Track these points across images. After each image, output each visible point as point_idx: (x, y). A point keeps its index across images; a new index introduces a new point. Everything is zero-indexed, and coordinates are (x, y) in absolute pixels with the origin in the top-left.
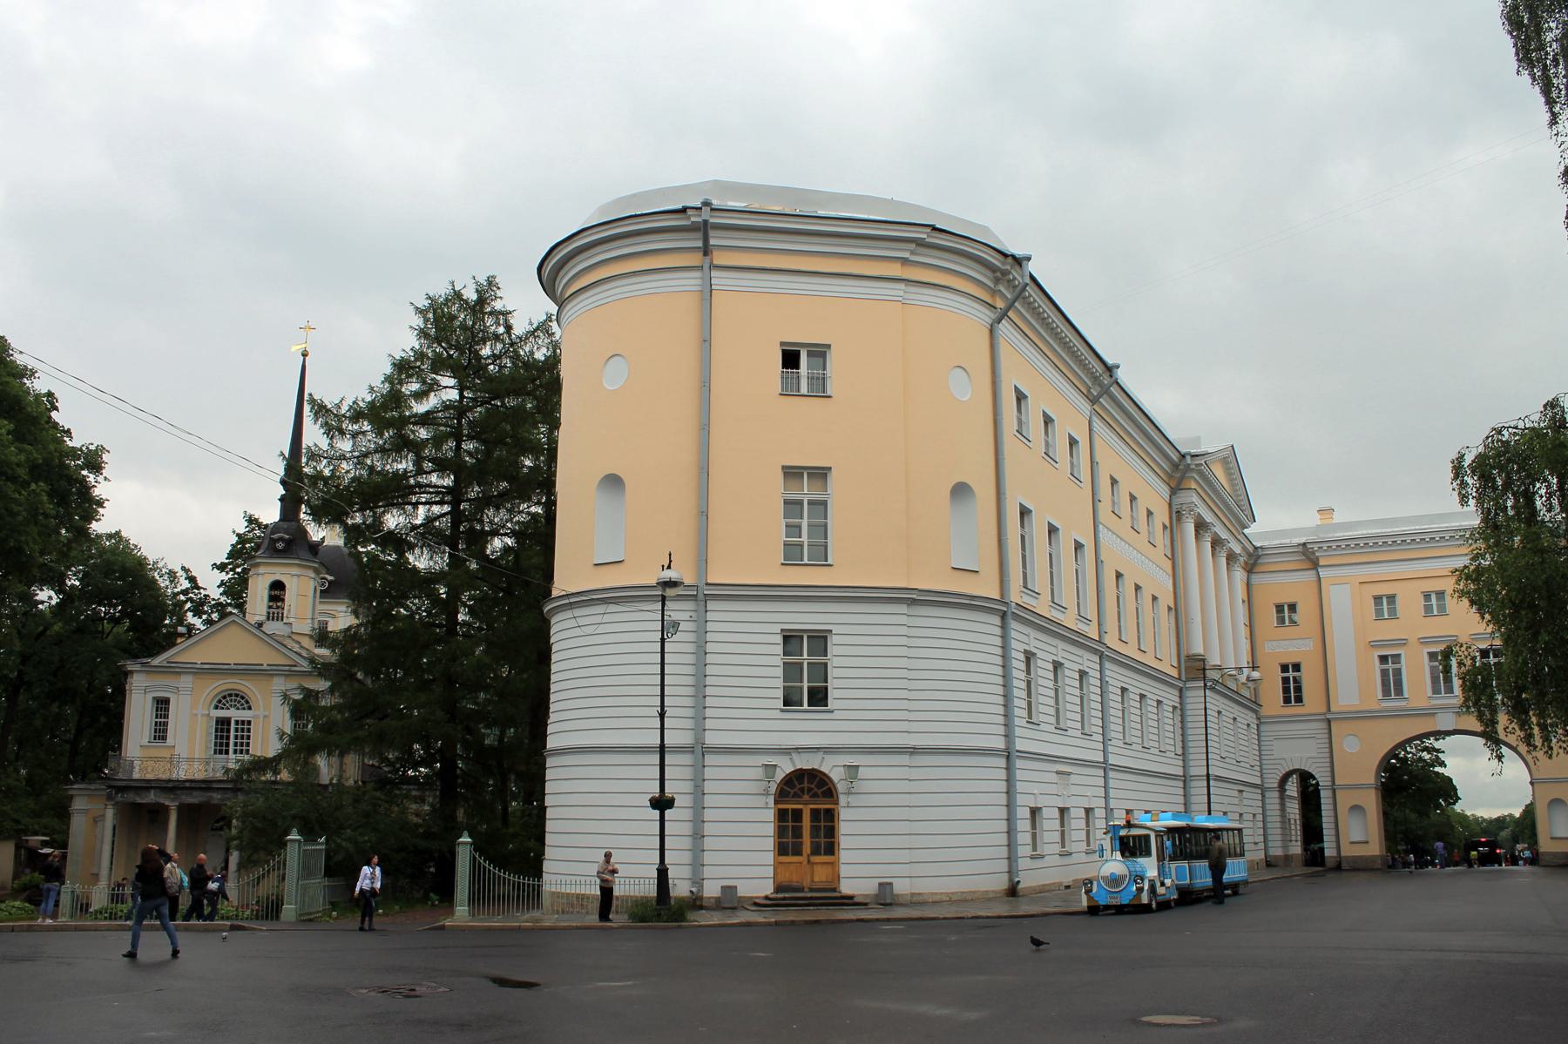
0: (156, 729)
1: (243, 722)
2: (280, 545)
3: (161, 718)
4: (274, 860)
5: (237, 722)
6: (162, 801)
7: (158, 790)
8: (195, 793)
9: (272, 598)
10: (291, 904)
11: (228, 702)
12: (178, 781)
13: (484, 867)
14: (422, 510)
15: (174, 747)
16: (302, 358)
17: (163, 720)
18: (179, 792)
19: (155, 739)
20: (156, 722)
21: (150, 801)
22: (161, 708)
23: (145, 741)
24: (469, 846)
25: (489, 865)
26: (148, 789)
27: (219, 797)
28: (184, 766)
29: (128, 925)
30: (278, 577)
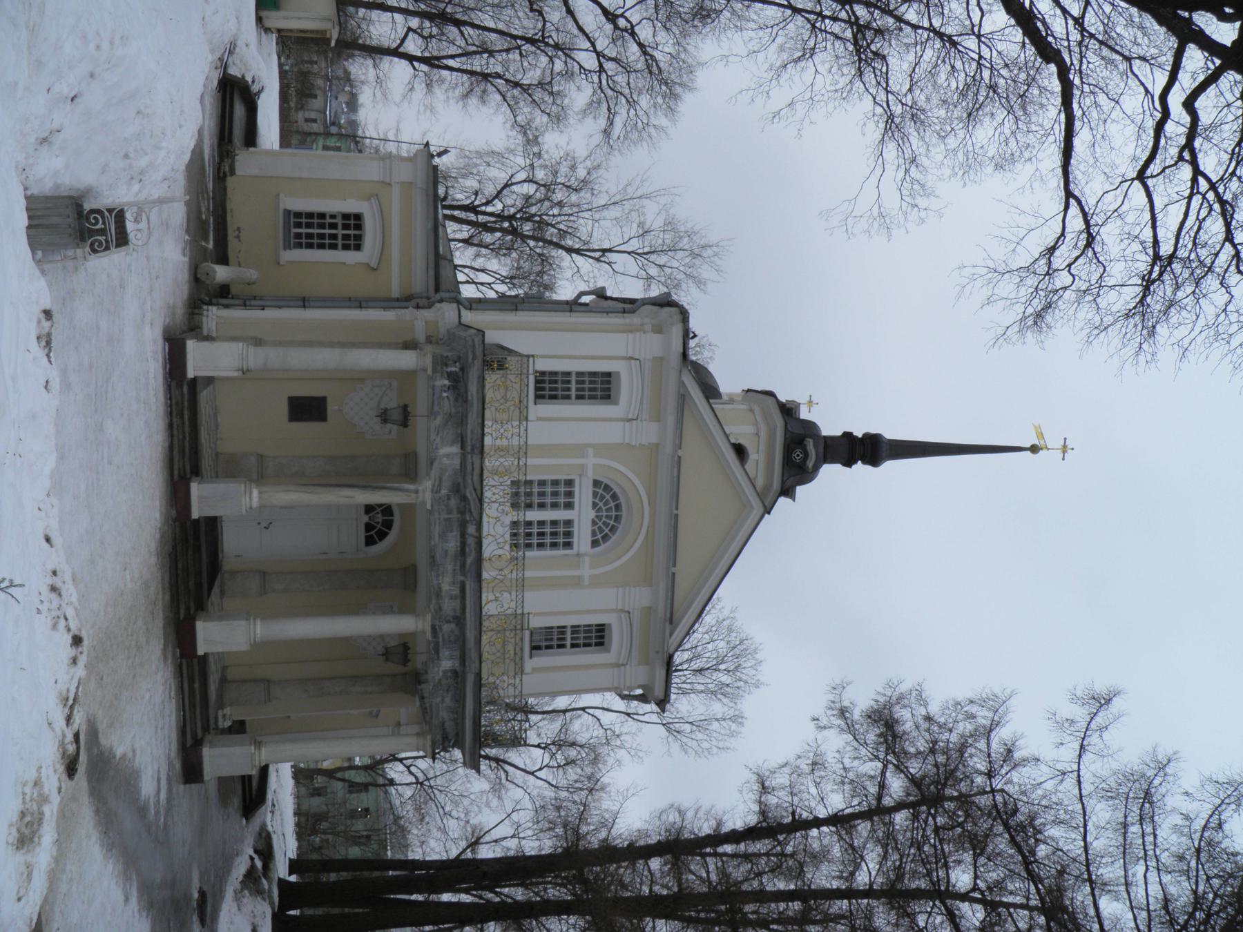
2: (797, 456)
5: (569, 523)
18: (453, 502)
27: (445, 587)
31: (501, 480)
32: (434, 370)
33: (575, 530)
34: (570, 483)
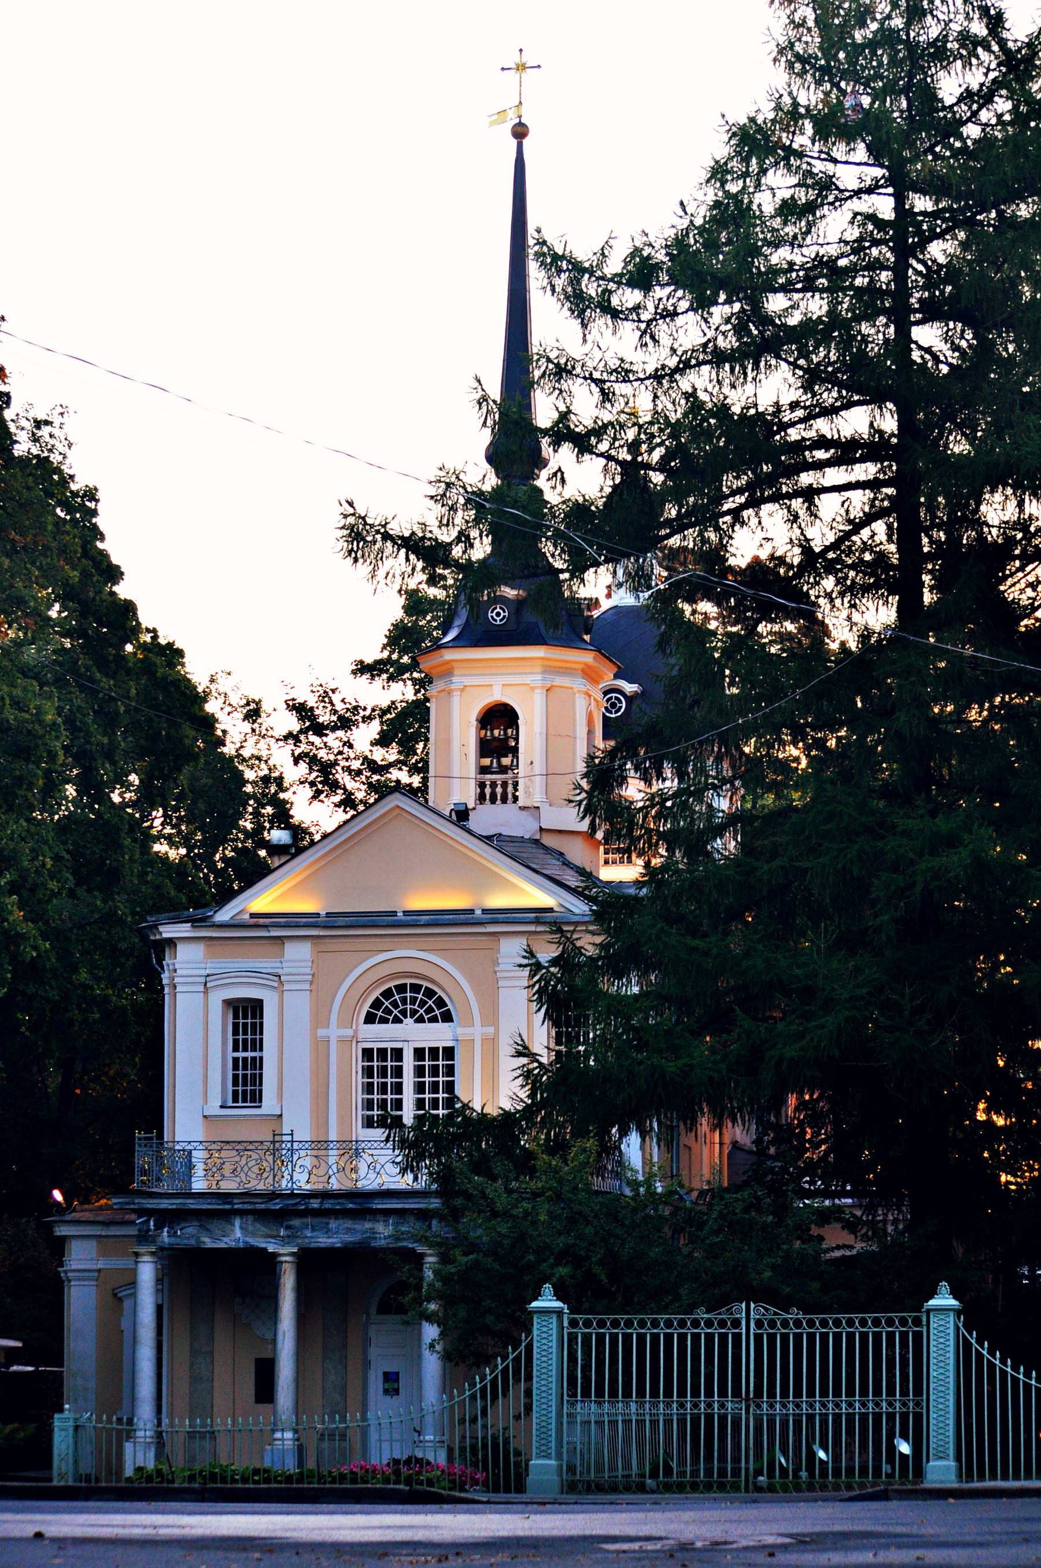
0: (235, 1077)
1: (434, 1052)
3: (245, 1050)
4: (505, 1358)
5: (419, 1053)
6: (260, 1243)
7: (250, 1218)
8: (333, 1224)
9: (486, 748)
10: (548, 1456)
11: (396, 1006)
12: (292, 1195)
13: (992, 1366)
14: (829, 505)
15: (281, 1115)
16: (514, 142)
17: (249, 1054)
18: (296, 1222)
19: (235, 1099)
20: (235, 1060)
21: (233, 1244)
22: (245, 1025)
23: (214, 1107)
24: (952, 1319)
25: (1003, 1361)
26: (226, 1216)
28: (305, 1160)
29: (194, 1488)
30: (497, 695)
31: (268, 1169)
32: (154, 1242)
33: (426, 1045)
34: (367, 1054)
